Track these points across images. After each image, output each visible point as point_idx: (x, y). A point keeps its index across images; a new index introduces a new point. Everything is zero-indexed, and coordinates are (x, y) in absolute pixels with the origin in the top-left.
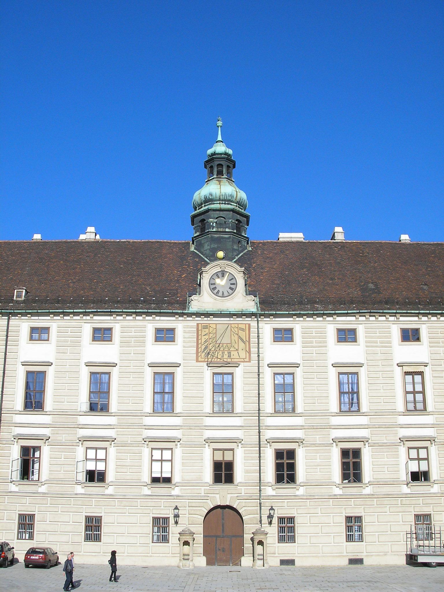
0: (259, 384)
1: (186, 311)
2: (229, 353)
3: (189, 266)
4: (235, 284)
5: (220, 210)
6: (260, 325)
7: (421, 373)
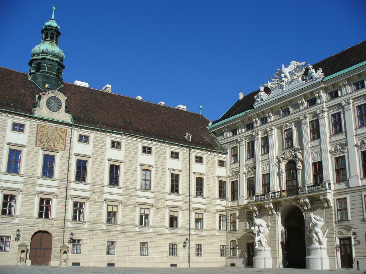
0: (69, 164)
1: (33, 116)
2: (54, 144)
3: (29, 89)
4: (61, 105)
5: (51, 60)
6: (72, 131)
7: (150, 171)
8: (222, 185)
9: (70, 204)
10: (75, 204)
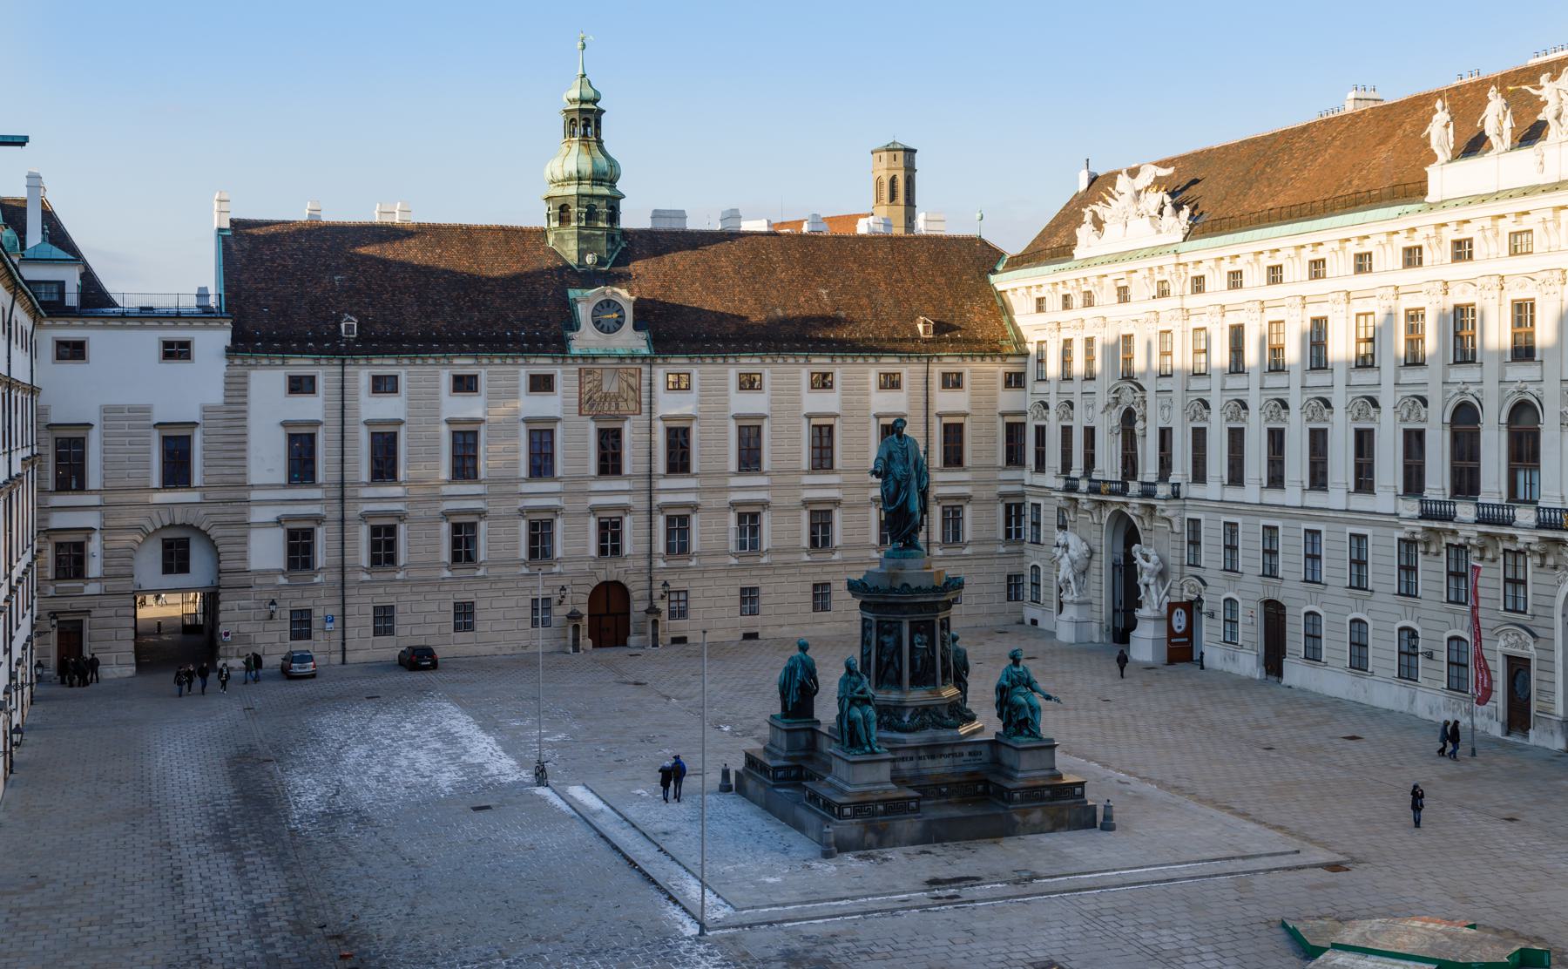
4: (622, 317)
8: (1014, 432)
9: (660, 522)
10: (670, 520)
